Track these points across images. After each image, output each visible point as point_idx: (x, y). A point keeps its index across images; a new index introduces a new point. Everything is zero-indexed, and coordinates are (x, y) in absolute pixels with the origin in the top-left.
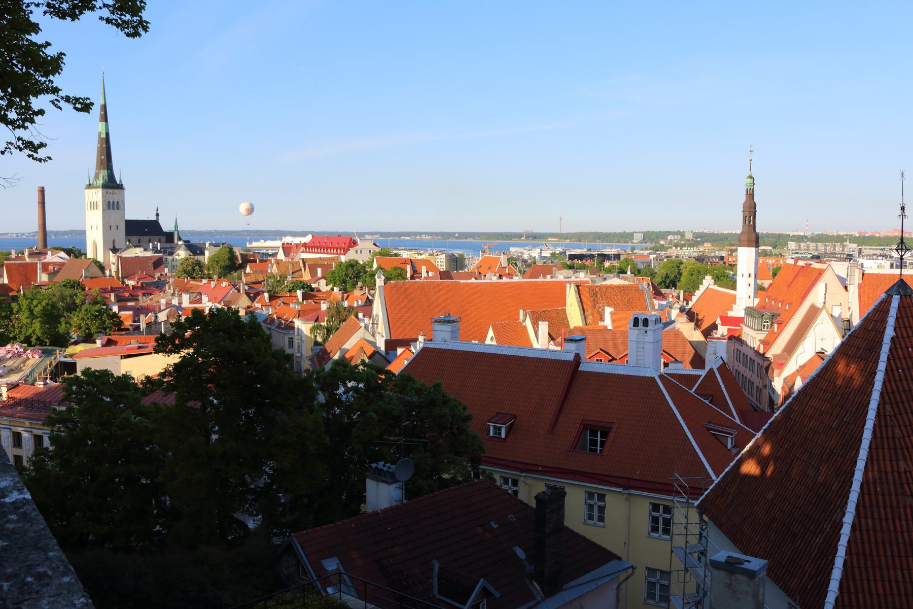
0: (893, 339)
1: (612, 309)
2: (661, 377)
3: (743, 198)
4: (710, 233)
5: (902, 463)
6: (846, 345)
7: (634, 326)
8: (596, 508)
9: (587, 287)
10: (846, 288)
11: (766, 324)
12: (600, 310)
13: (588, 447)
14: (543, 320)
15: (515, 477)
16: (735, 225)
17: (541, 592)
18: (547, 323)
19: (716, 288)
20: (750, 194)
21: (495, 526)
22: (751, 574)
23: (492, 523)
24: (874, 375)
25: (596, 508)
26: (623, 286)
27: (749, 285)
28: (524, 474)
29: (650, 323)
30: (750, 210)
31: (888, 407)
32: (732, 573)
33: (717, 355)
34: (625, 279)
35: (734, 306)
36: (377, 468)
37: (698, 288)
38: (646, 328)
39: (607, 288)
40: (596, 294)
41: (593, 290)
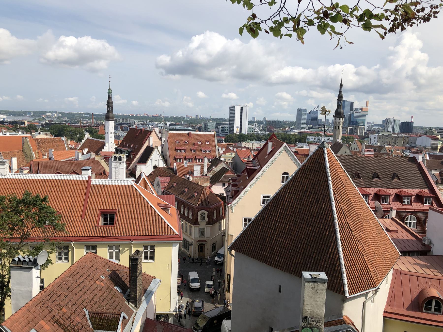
0: (329, 166)
1: (53, 150)
2: (134, 184)
3: (107, 99)
4: (120, 115)
5: (347, 218)
6: (302, 169)
7: (114, 160)
8: (114, 253)
9: (34, 139)
10: (161, 139)
11: (127, 154)
12: (42, 150)
13: (103, 223)
14: (15, 156)
15: (66, 245)
16: (103, 110)
17: (135, 308)
18: (16, 158)
19: (91, 138)
20: (110, 98)
21: (103, 278)
22: (323, 281)
23: (101, 277)
24: (326, 183)
25: (114, 253)
26: (46, 139)
27: (111, 137)
28: (73, 243)
29: (122, 159)
30: (109, 104)
31: (336, 196)
32: (315, 282)
33: (141, 171)
34: (47, 135)
35: (105, 147)
36: (19, 260)
37: (83, 139)
38: (120, 161)
39: (45, 140)
40: (39, 143)
41: (37, 141)
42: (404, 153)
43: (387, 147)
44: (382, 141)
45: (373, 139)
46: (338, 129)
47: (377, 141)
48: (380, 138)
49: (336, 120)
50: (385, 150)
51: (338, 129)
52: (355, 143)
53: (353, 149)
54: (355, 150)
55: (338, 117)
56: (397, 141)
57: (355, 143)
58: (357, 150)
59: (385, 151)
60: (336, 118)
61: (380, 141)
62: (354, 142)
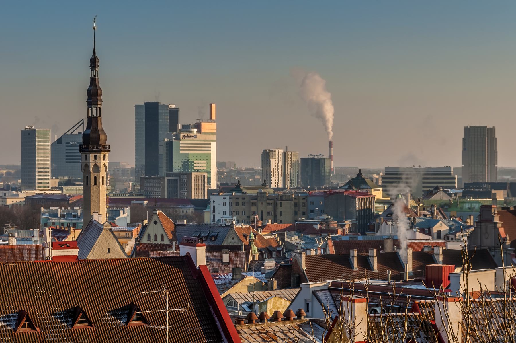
42: (286, 239)
43: (238, 226)
44: (244, 213)
45: (220, 209)
46: (95, 184)
47: (231, 213)
48: (237, 204)
49: (86, 159)
50: (234, 236)
51: (95, 184)
52: (155, 223)
53: (152, 238)
54: (159, 242)
55: (92, 152)
56: (279, 209)
57: (155, 223)
58: (162, 240)
59: (236, 240)
60: (87, 153)
61: (237, 213)
62: (155, 218)
